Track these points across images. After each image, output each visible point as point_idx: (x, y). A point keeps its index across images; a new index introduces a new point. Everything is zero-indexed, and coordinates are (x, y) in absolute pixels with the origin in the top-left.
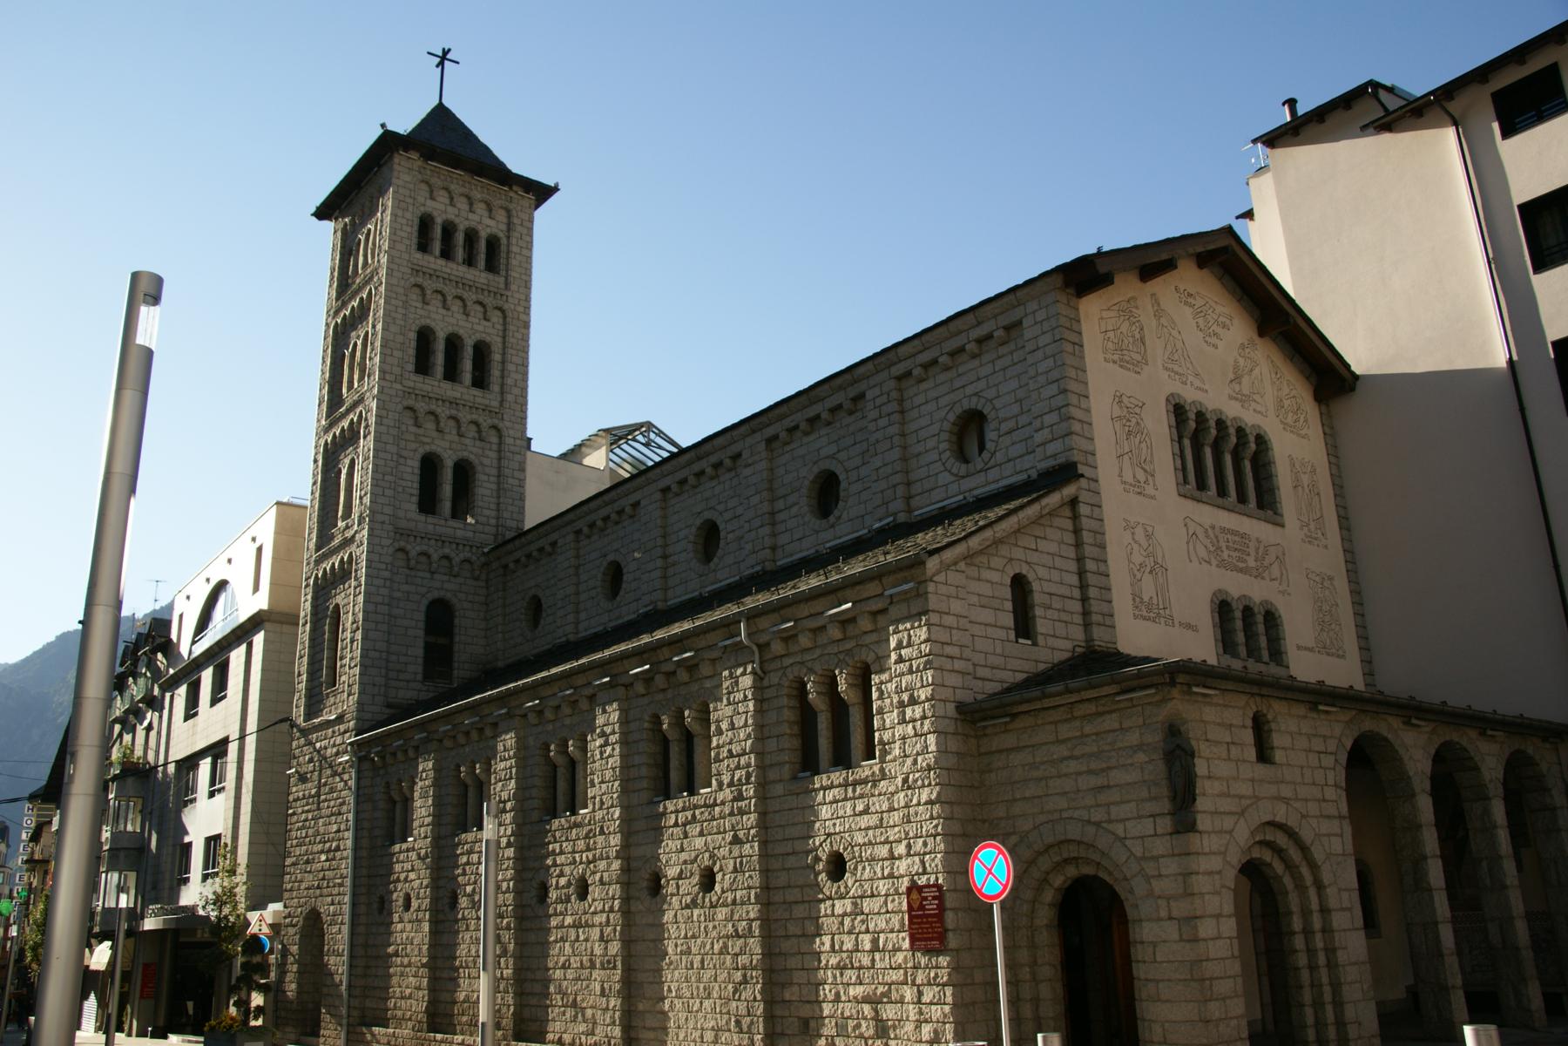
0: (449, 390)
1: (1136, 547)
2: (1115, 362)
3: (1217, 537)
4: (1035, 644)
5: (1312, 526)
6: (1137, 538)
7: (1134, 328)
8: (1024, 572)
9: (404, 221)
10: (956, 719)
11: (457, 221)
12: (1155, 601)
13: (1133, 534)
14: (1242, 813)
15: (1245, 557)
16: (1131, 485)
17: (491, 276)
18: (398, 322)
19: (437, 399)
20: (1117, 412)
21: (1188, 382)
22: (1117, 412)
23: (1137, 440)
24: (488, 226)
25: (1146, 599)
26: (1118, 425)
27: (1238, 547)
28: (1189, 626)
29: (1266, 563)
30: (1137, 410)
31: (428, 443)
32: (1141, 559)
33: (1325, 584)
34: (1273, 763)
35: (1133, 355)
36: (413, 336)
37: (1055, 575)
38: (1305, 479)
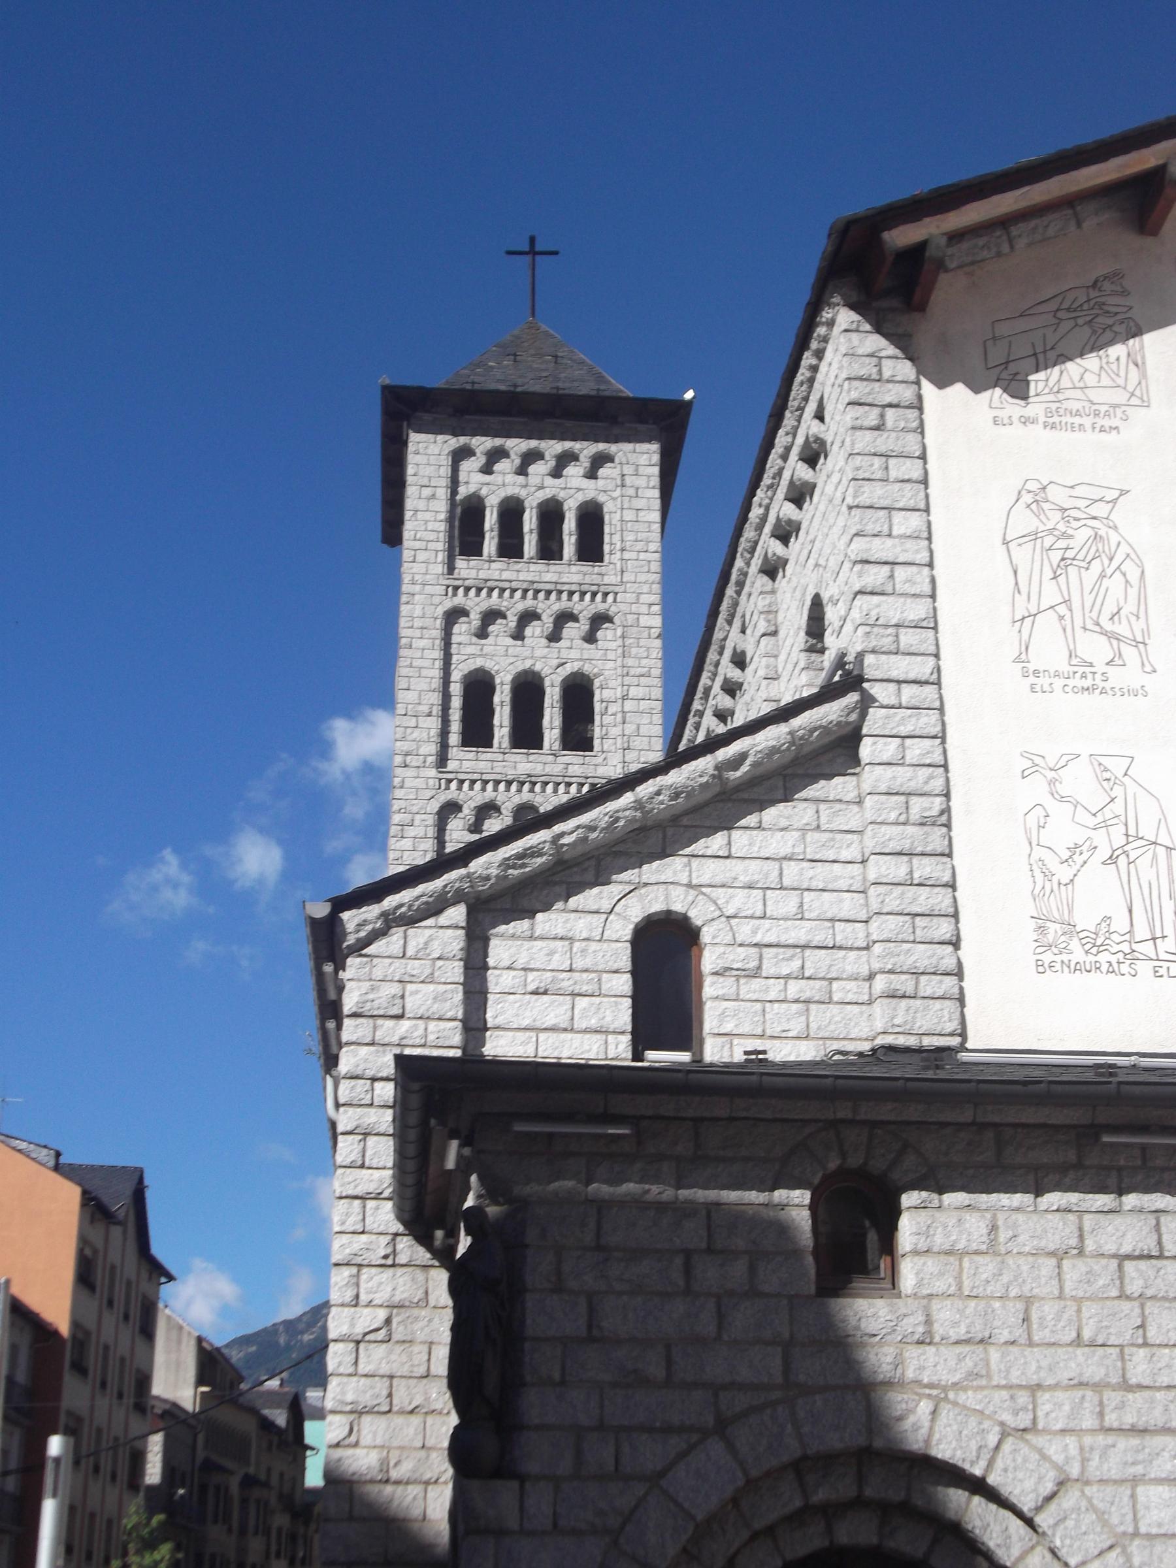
0: (523, 763)
2: (1026, 421)
6: (1063, 789)
7: (1108, 335)
8: (678, 907)
9: (428, 516)
10: (396, 1235)
11: (523, 493)
12: (1120, 923)
13: (1052, 782)
14: (722, 1427)
16: (1057, 675)
17: (586, 567)
18: (424, 672)
19: (497, 783)
20: (1025, 520)
22: (1025, 520)
24: (579, 490)
25: (1085, 920)
26: (1022, 555)
30: (1100, 510)
32: (1080, 836)
34: (899, 1296)
35: (1103, 396)
36: (456, 689)
37: (786, 904)
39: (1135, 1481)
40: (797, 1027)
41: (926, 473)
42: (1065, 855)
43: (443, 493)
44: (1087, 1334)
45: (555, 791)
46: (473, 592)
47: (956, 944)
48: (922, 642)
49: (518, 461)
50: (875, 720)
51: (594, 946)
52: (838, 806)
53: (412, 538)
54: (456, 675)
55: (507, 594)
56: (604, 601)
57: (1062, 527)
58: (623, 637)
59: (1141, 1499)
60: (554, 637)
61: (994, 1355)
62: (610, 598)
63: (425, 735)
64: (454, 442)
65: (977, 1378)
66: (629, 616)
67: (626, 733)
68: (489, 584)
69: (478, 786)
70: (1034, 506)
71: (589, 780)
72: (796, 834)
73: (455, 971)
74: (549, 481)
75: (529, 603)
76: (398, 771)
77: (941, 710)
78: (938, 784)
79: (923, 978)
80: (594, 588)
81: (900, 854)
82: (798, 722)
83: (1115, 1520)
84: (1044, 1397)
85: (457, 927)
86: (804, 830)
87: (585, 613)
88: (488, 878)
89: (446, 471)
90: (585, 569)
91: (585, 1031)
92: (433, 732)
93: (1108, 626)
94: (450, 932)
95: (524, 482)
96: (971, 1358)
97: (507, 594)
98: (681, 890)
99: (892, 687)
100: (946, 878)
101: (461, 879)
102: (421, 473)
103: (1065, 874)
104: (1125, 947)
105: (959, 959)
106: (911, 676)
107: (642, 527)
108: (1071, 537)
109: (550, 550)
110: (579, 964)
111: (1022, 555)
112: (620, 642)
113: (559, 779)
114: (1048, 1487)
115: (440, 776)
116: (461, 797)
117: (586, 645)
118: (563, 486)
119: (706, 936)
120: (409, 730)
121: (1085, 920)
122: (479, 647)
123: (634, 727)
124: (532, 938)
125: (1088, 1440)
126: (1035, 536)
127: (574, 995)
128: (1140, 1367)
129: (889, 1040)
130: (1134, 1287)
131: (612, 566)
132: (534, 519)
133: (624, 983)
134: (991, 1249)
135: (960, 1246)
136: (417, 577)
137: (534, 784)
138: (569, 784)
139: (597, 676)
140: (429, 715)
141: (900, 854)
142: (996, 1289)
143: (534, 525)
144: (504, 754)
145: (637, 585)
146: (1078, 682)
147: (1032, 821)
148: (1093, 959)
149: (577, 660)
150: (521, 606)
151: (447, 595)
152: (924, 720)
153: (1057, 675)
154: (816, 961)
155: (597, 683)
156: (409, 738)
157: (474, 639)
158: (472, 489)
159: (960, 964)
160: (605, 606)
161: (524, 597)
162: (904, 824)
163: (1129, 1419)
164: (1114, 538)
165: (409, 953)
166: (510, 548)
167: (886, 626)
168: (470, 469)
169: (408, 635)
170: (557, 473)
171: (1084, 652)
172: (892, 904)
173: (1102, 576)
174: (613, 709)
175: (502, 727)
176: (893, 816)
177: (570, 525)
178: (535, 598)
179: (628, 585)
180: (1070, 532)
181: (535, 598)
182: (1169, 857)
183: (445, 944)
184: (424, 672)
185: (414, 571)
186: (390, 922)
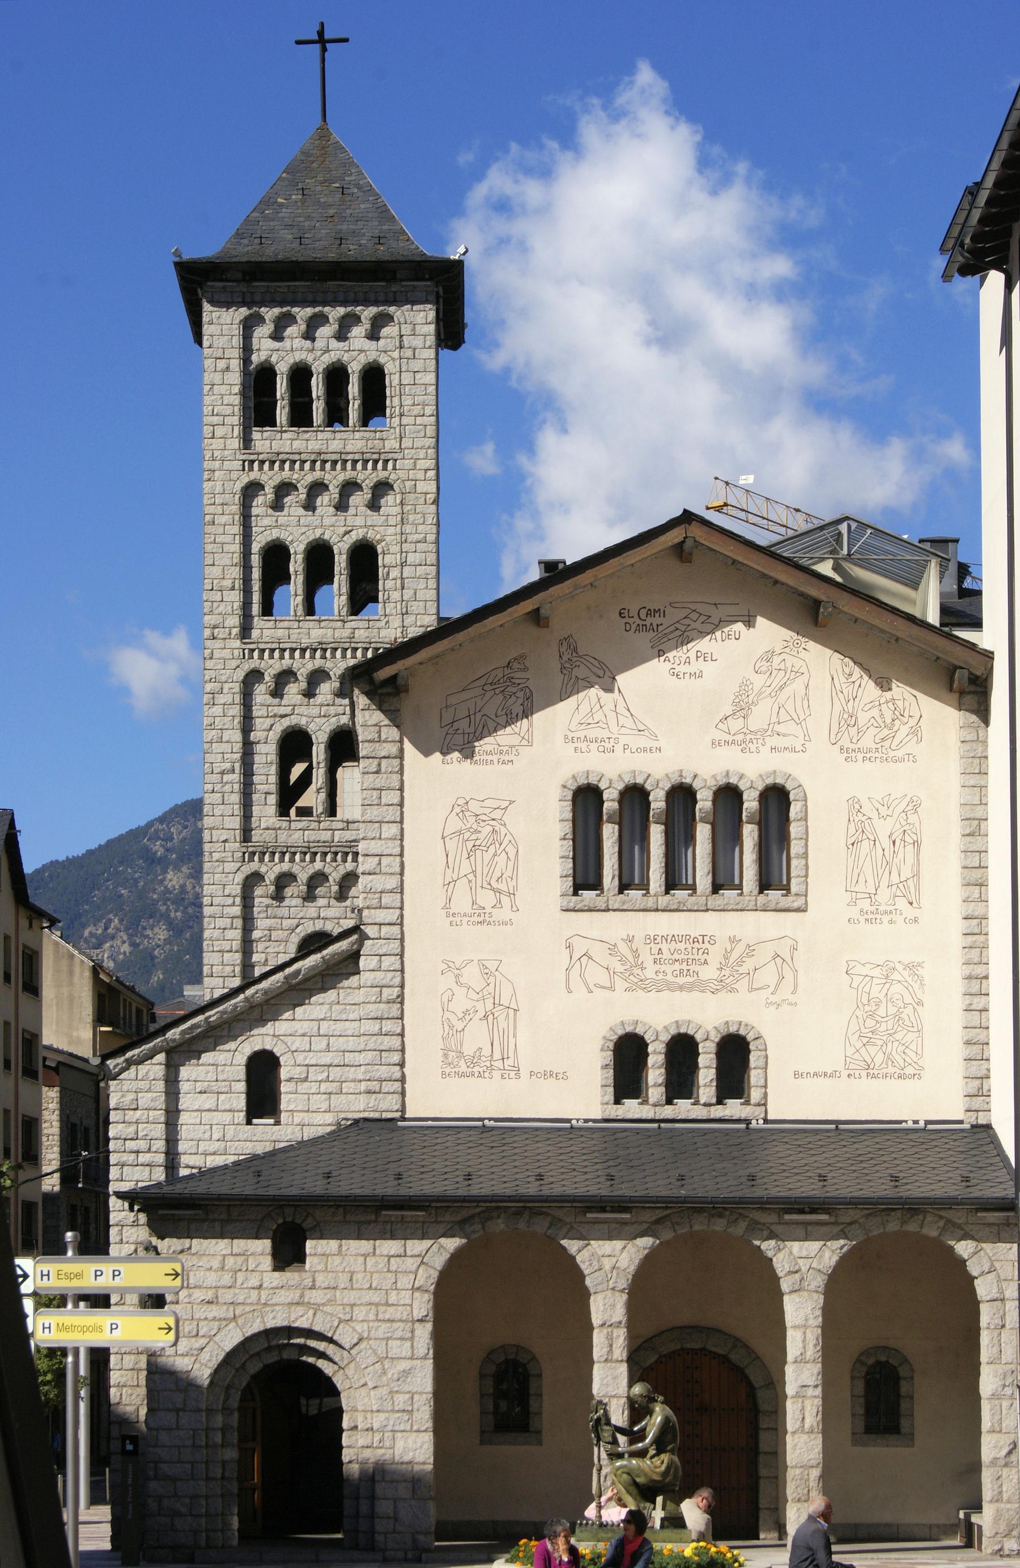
1: (461, 992)
3: (636, 953)
4: (278, 1123)
5: (884, 895)
6: (462, 980)
8: (268, 1047)
9: (224, 389)
11: (310, 358)
13: (457, 976)
15: (692, 968)
16: (465, 915)
19: (293, 650)
20: (455, 824)
21: (619, 748)
22: (455, 824)
23: (488, 856)
25: (469, 1050)
26: (451, 845)
27: (683, 956)
28: (549, 1074)
29: (741, 970)
31: (286, 716)
32: (469, 1005)
33: (895, 976)
36: (256, 560)
37: (320, 1044)
38: (883, 829)
39: (388, 1339)
40: (324, 1106)
41: (402, 797)
42: (461, 1015)
43: (236, 364)
44: (374, 1285)
45: (344, 656)
46: (266, 466)
47: (402, 1065)
48: (393, 901)
49: (303, 327)
50: (368, 946)
51: (227, 1068)
52: (349, 990)
53: (210, 413)
54: (256, 547)
55: (297, 466)
56: (385, 468)
57: (475, 826)
58: (402, 504)
59: (390, 1344)
60: (341, 506)
61: (338, 1293)
62: (390, 465)
63: (229, 608)
64: (244, 312)
65: (330, 1302)
66: (407, 483)
67: (405, 598)
68: (281, 457)
69: (277, 654)
70: (461, 815)
71: (373, 645)
72: (327, 1007)
73: (161, 1085)
74: (334, 344)
75: (318, 474)
76: (208, 643)
77: (402, 940)
78: (397, 981)
79: (384, 1083)
80: (376, 456)
81: (376, 1019)
82: (325, 952)
83: (379, 1352)
84: (356, 1308)
85: (161, 1064)
86: (331, 1004)
87: (367, 482)
88: (174, 1040)
89: (237, 341)
90: (367, 435)
91: (224, 1111)
92: (236, 605)
93: (495, 885)
94: (158, 1067)
95: (311, 347)
96: (330, 1294)
97: (297, 466)
98: (270, 1038)
99: (376, 927)
100: (399, 1031)
101: (162, 1041)
102: (215, 345)
103: (459, 1026)
104: (488, 1064)
105: (403, 1072)
106: (387, 921)
107: (419, 390)
108: (480, 832)
109: (336, 415)
110: (220, 1078)
111: (451, 845)
112: (398, 509)
113: (347, 645)
114: (355, 1341)
115: (244, 646)
116: (262, 666)
117: (369, 512)
118: (346, 348)
119: (282, 1060)
120: (215, 605)
121: (469, 1050)
122: (274, 519)
123: (412, 592)
124: (198, 1065)
125: (371, 1324)
126: (460, 833)
127: (218, 1093)
128: (393, 1298)
129: (366, 1115)
130: (393, 1268)
131: (392, 430)
132: (320, 385)
133: (242, 1086)
134: (340, 1253)
135: (328, 1252)
136: (216, 454)
137: (325, 650)
138: (355, 650)
139: (379, 542)
140: (233, 589)
141: (376, 1019)
142: (340, 1268)
143: (321, 392)
144: (299, 621)
145: (414, 451)
146: (476, 919)
147: (445, 999)
148: (470, 1070)
149: (361, 527)
150: (310, 478)
151: (244, 470)
152: (392, 945)
153: (465, 915)
154: (335, 1073)
155: (379, 550)
156: (216, 612)
157: (270, 511)
158: (263, 358)
159: (403, 1076)
160: (385, 474)
161: (312, 468)
162: (380, 1002)
163: (387, 1317)
164: (503, 831)
165: (139, 1077)
166: (301, 417)
167: (375, 893)
168: (262, 334)
169: (211, 511)
170: (341, 336)
171: (481, 902)
172: (371, 1046)
173: (495, 855)
174: (395, 573)
175: (296, 595)
176: (374, 998)
177: (354, 389)
178: (323, 469)
179: (406, 452)
180: (479, 829)
181: (323, 469)
182: (515, 1015)
183: (155, 1073)
184: (226, 548)
185: (213, 447)
186: (129, 1063)
